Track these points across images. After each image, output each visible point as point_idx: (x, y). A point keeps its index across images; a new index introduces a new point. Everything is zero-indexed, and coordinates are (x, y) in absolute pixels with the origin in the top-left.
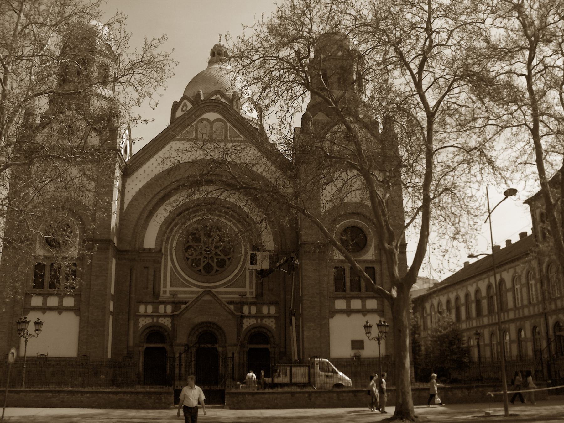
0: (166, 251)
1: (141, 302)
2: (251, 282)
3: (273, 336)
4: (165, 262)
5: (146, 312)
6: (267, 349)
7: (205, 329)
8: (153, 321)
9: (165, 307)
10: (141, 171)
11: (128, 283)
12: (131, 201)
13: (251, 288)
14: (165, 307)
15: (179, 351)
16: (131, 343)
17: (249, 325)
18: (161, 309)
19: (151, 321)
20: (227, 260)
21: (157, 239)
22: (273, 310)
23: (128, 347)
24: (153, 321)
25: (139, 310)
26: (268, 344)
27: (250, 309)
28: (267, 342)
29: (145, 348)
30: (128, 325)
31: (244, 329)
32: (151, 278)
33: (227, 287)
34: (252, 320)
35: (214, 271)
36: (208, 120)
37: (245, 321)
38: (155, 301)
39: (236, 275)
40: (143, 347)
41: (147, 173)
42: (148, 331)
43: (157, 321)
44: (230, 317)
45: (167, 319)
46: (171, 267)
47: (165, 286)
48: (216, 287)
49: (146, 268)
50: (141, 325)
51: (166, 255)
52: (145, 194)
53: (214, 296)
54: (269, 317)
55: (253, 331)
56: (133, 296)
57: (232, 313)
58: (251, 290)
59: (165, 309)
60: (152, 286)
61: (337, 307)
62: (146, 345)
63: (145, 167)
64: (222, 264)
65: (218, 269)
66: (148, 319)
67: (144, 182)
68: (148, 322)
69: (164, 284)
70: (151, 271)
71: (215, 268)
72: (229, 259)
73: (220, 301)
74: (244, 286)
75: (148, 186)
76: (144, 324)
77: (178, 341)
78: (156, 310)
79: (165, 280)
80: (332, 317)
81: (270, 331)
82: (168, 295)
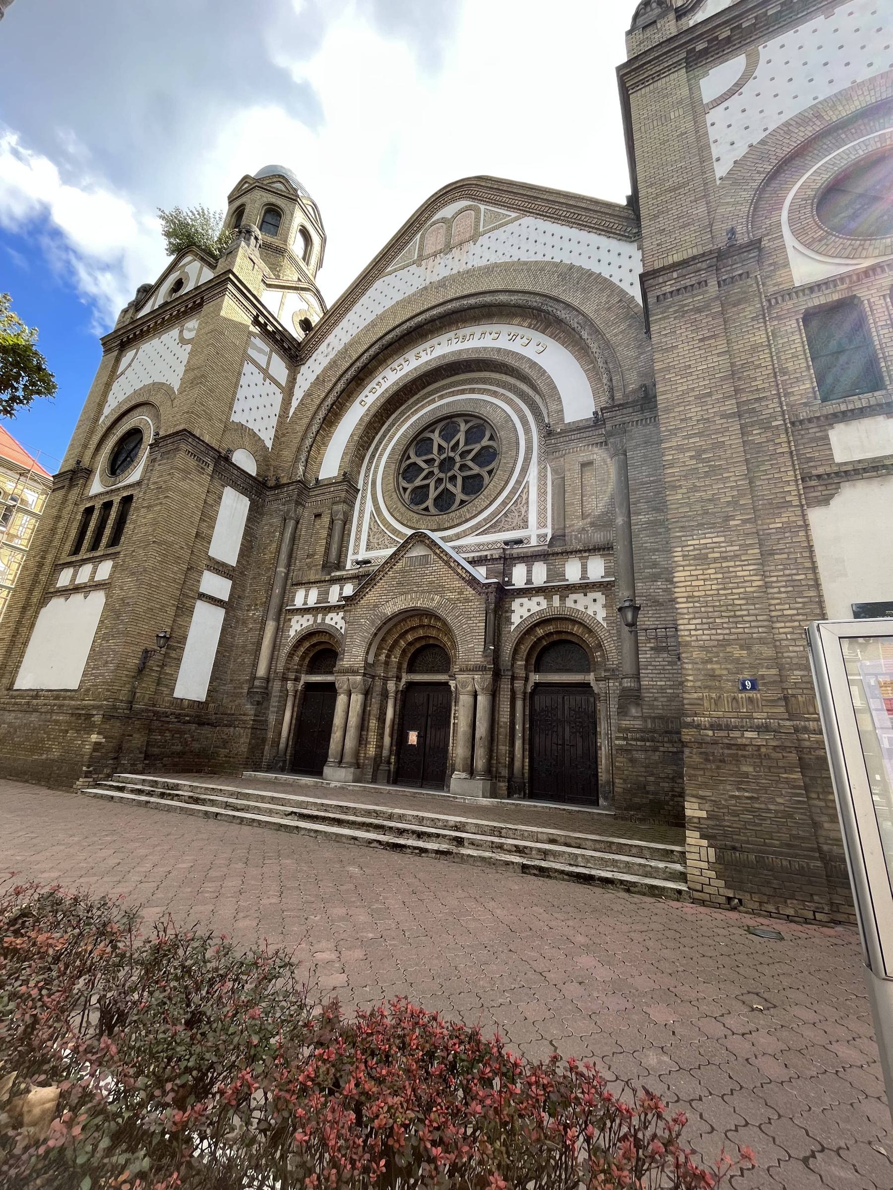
0: (365, 484)
1: (299, 584)
2: (542, 512)
3: (600, 646)
4: (362, 503)
6: (585, 687)
7: (421, 633)
10: (323, 347)
11: (274, 545)
12: (302, 400)
13: (542, 524)
15: (345, 687)
16: (261, 671)
18: (334, 595)
20: (486, 475)
21: (342, 458)
22: (597, 569)
23: (254, 678)
24: (315, 621)
25: (293, 601)
26: (588, 671)
27: (529, 572)
28: (585, 663)
30: (262, 629)
31: (513, 627)
32: (324, 533)
34: (535, 599)
35: (458, 502)
36: (443, 220)
37: (515, 605)
39: (504, 503)
40: (297, 679)
41: (331, 348)
42: (307, 645)
43: (324, 619)
44: (469, 592)
46: (372, 513)
48: (458, 537)
49: (318, 516)
50: (292, 633)
51: (365, 490)
52: (324, 381)
53: (432, 545)
54: (585, 587)
55: (540, 632)
57: (473, 582)
58: (543, 531)
61: (839, 457)
63: (330, 338)
64: (474, 485)
65: (465, 498)
66: (306, 617)
67: (325, 362)
70: (326, 520)
71: (460, 496)
72: (490, 472)
74: (525, 524)
75: (333, 364)
76: (299, 629)
77: (346, 662)
78: (324, 596)
79: (358, 539)
80: (825, 501)
81: (590, 631)
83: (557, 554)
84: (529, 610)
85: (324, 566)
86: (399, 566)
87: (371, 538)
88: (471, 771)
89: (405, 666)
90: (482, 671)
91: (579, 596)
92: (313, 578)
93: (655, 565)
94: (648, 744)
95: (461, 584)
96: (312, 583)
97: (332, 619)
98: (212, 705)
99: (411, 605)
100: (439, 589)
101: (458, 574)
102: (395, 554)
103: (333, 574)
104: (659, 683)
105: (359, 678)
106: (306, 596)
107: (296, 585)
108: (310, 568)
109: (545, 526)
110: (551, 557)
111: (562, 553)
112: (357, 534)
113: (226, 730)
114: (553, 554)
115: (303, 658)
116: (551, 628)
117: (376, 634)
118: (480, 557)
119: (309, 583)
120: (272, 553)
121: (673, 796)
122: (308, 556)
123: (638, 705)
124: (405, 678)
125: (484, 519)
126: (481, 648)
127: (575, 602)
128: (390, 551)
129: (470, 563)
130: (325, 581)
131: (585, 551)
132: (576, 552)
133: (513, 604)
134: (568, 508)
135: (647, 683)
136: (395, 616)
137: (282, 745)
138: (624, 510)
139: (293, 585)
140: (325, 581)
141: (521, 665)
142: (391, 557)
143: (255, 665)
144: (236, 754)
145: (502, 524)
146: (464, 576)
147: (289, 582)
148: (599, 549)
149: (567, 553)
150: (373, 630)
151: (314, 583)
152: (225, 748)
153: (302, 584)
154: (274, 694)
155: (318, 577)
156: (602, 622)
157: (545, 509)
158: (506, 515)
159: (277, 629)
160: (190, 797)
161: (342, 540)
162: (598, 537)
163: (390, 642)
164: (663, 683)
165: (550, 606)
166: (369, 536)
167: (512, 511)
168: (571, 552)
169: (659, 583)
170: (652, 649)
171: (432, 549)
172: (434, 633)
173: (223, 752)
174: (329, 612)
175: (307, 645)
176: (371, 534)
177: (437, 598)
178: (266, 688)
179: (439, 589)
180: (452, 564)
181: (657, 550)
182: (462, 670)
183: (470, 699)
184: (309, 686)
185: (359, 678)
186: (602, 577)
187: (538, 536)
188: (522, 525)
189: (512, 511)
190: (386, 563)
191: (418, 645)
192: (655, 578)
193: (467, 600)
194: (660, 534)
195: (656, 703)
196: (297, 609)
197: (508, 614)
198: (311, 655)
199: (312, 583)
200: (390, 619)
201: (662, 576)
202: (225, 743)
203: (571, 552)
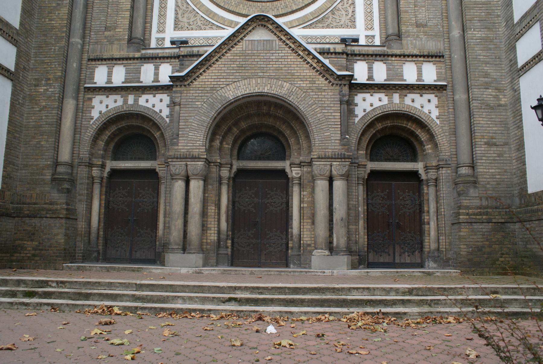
2: (369, 14)
5: (109, 81)
6: (414, 175)
7: (256, 121)
8: (125, 102)
9: (157, 68)
11: (65, 11)
14: (157, 68)
15: (183, 173)
16: (65, 155)
17: (369, 109)
19: (120, 102)
23: (57, 164)
24: (125, 102)
25: (93, 78)
27: (370, 69)
29: (108, 169)
30: (61, 109)
31: (357, 120)
33: (310, 26)
34: (377, 96)
37: (359, 98)
38: (131, 55)
40: (103, 166)
42: (113, 128)
43: (136, 101)
44: (321, 81)
45: (159, 96)
47: (161, 30)
50: (95, 114)
55: (379, 126)
56: (76, 40)
57: (326, 71)
58: (370, 33)
59: (156, 74)
60: (127, 22)
62: (111, 165)
66: (112, 97)
68: (112, 105)
69: (159, 23)
73: (295, 41)
74: (352, 24)
76: (104, 110)
79: (162, 15)
82: (168, 44)
83: (396, 56)
84: (372, 105)
85: (130, 40)
86: (238, 49)
87: (179, 16)
88: (331, 249)
89: (235, 152)
90: (341, 158)
91: (416, 96)
92: (117, 54)
93: (487, 75)
94: (484, 217)
95: (312, 73)
96: (116, 59)
97: (147, 101)
98: (7, 193)
99: (257, 91)
100: (290, 77)
101: (308, 63)
102: (234, 35)
103: (143, 52)
104: (490, 171)
105: (200, 164)
106: (110, 74)
107: (95, 60)
108: (112, 43)
109: (372, 28)
110: (390, 58)
111: (400, 56)
112: (160, 12)
113: (27, 220)
114: (392, 56)
115: (107, 143)
116: (389, 123)
117: (215, 118)
118: (323, 49)
119: (112, 59)
120: (62, 19)
121: (503, 254)
122: (107, 29)
123: (475, 187)
124: (237, 165)
125: (311, 13)
126: (338, 137)
127: (413, 101)
128: (229, 32)
129: (320, 53)
130: (134, 59)
131: (420, 56)
132: (413, 56)
133: (356, 98)
134: (403, 15)
135: (482, 170)
136: (237, 100)
137: (93, 235)
138: (460, 25)
139: (89, 60)
140: (134, 59)
141: (362, 154)
142: (229, 39)
143: (57, 148)
144: (50, 247)
145: (330, 19)
146: (315, 65)
147: (85, 56)
148: (432, 57)
149: (404, 56)
150: (213, 113)
151: (119, 59)
152: (32, 240)
153: (102, 59)
154: (79, 182)
155: (124, 53)
156: (435, 119)
157: (371, 12)
158: (332, 12)
159: (77, 109)
160: (75, 293)
161: (146, 16)
162: (432, 46)
163: (224, 128)
164: (493, 171)
165: (391, 101)
166: (177, 14)
167: (339, 10)
168: (408, 56)
169: (490, 91)
170: (486, 143)
171: (275, 34)
172: (270, 121)
173: (29, 245)
174: (143, 93)
175: (113, 128)
176: (180, 13)
177: (286, 85)
178: (71, 174)
179: (290, 77)
180: (300, 53)
181: (488, 63)
182: (320, 158)
183: (326, 183)
184: (114, 173)
185: (200, 164)
186: (435, 81)
187: (367, 36)
188: (350, 24)
189: (339, 10)
190: (224, 43)
191: (249, 134)
192: (487, 86)
193: (319, 89)
194: (490, 49)
195: (488, 186)
196: (100, 89)
197: (352, 107)
198: (116, 140)
199: (116, 59)
200: (232, 103)
201: (492, 85)
202: (31, 235)
203: (408, 56)
